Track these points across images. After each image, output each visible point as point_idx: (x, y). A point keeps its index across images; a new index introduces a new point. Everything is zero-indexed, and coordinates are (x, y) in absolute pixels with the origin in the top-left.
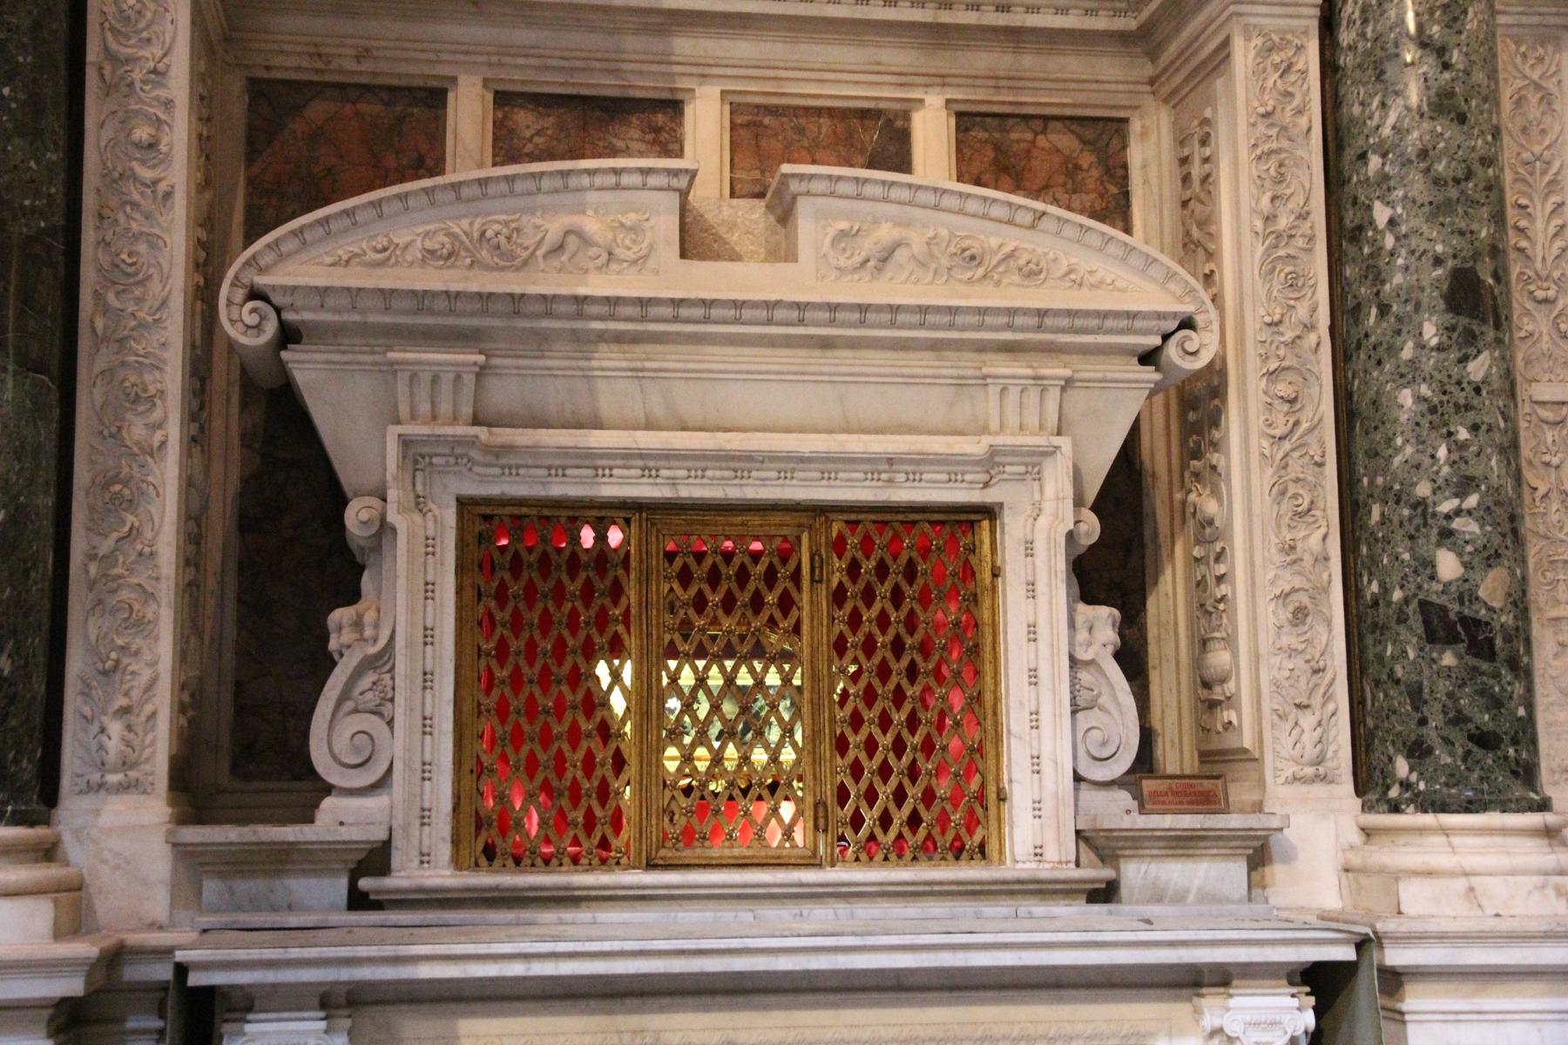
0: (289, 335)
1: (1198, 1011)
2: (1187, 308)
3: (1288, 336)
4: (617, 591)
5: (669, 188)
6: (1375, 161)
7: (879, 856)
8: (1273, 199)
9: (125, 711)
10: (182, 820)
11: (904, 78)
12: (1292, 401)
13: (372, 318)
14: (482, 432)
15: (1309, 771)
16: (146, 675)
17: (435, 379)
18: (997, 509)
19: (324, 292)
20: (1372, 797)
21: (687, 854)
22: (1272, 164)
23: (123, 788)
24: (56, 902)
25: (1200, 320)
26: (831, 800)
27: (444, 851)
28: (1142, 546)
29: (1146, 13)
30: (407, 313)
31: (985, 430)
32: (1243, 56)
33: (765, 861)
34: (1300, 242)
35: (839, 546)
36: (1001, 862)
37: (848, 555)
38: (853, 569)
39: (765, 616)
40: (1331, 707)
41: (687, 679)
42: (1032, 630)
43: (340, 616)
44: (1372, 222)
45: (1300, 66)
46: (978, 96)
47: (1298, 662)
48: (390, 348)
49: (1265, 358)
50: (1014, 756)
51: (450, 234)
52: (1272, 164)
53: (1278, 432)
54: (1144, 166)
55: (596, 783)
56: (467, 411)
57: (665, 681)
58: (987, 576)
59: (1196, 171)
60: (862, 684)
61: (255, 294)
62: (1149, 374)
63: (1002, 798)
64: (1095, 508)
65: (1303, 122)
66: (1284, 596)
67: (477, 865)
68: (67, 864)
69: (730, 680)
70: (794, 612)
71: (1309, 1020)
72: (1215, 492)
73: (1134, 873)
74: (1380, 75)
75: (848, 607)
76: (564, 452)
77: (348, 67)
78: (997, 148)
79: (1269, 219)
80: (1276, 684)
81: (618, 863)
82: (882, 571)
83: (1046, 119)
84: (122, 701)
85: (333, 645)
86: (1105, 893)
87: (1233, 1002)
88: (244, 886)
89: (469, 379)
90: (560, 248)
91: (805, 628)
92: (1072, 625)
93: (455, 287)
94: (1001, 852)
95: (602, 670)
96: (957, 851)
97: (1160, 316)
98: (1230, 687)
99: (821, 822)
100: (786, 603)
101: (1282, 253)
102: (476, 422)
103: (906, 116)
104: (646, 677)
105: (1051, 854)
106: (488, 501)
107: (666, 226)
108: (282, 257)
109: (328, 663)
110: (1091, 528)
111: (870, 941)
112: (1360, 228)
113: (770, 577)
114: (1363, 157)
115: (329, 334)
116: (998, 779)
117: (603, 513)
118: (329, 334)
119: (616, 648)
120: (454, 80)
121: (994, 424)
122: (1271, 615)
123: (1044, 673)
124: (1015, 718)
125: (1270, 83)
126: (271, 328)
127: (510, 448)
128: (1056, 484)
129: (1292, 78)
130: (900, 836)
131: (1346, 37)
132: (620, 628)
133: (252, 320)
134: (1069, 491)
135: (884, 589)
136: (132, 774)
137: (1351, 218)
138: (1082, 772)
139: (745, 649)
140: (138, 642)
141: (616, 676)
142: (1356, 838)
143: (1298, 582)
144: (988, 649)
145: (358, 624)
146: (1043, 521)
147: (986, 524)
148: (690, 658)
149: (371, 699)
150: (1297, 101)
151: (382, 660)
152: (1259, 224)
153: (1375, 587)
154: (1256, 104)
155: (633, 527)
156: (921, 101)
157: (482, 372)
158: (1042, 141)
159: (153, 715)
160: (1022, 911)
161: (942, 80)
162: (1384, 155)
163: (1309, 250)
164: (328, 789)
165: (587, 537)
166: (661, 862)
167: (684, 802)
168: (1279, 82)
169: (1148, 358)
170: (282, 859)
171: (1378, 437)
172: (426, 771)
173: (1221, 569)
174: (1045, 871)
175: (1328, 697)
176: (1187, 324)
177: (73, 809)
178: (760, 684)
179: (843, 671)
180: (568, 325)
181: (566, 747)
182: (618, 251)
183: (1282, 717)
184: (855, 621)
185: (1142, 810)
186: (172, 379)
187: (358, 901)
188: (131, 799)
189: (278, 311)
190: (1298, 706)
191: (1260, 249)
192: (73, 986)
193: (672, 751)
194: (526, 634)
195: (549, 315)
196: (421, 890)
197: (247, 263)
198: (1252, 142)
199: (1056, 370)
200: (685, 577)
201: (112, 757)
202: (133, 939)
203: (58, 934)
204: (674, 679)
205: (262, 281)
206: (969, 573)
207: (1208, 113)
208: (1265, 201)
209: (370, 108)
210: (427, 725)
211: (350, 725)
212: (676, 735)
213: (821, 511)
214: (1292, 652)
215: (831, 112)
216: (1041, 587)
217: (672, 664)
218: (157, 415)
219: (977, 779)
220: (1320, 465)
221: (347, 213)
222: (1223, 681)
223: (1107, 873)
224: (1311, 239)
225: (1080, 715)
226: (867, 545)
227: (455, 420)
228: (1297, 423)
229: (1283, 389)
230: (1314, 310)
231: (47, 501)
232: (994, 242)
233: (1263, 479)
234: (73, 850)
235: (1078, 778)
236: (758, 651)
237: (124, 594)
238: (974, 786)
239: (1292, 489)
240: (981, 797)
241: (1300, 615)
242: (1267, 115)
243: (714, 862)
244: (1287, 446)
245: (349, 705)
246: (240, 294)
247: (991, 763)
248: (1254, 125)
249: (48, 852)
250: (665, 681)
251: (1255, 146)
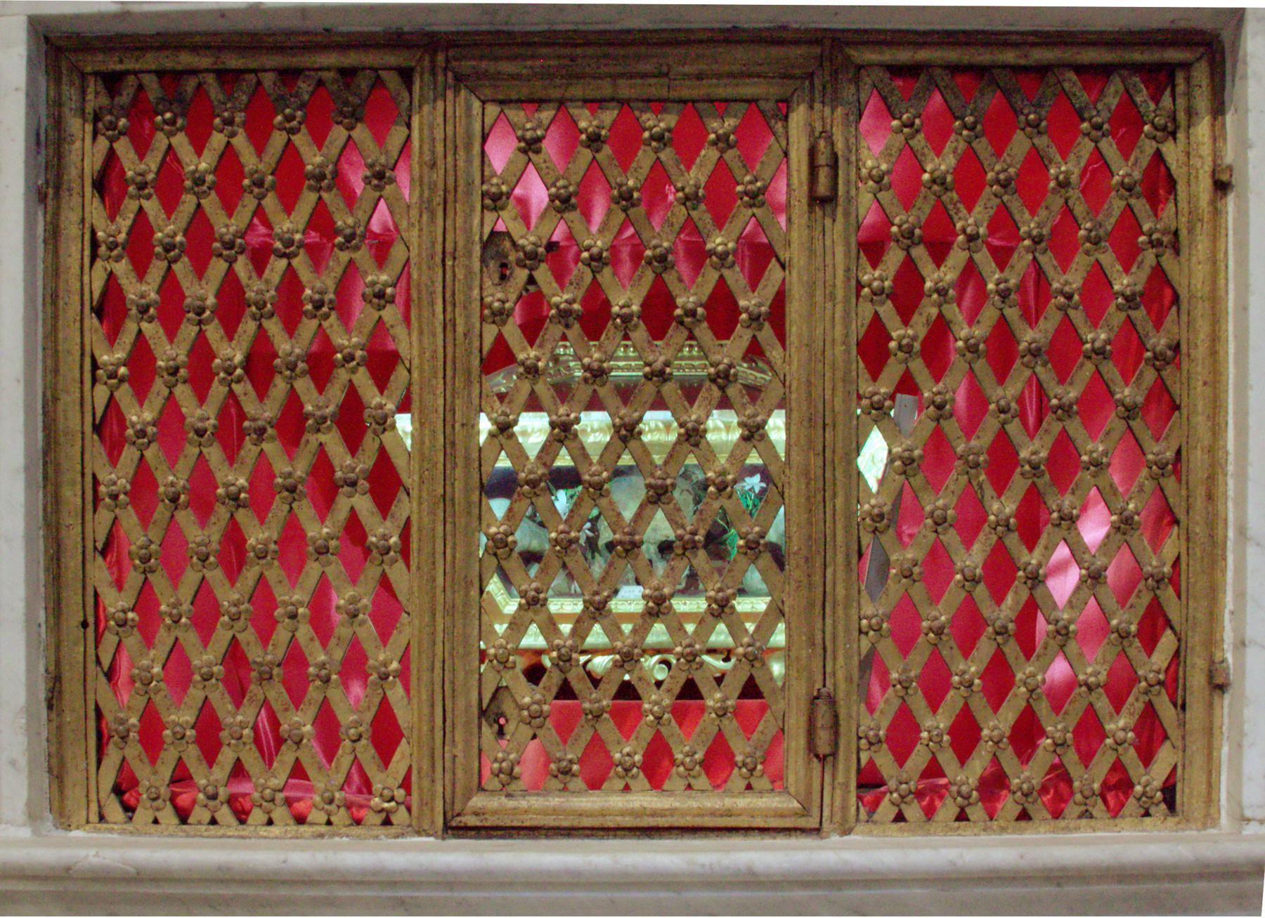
18: (1226, 36)
33: (698, 822)
36: (1210, 819)
50: (1252, 585)
55: (339, 654)
58: (1204, 187)
67: (102, 818)
70: (774, 274)
81: (387, 822)
94: (1210, 798)
99: (823, 737)
116: (1212, 641)
130: (933, 769)
144: (1201, 352)
147: (1201, 74)
155: (416, 87)
166: (472, 821)
167: (526, 695)
219: (1167, 642)
238: (1161, 657)
240: (1172, 682)
243: (587, 822)
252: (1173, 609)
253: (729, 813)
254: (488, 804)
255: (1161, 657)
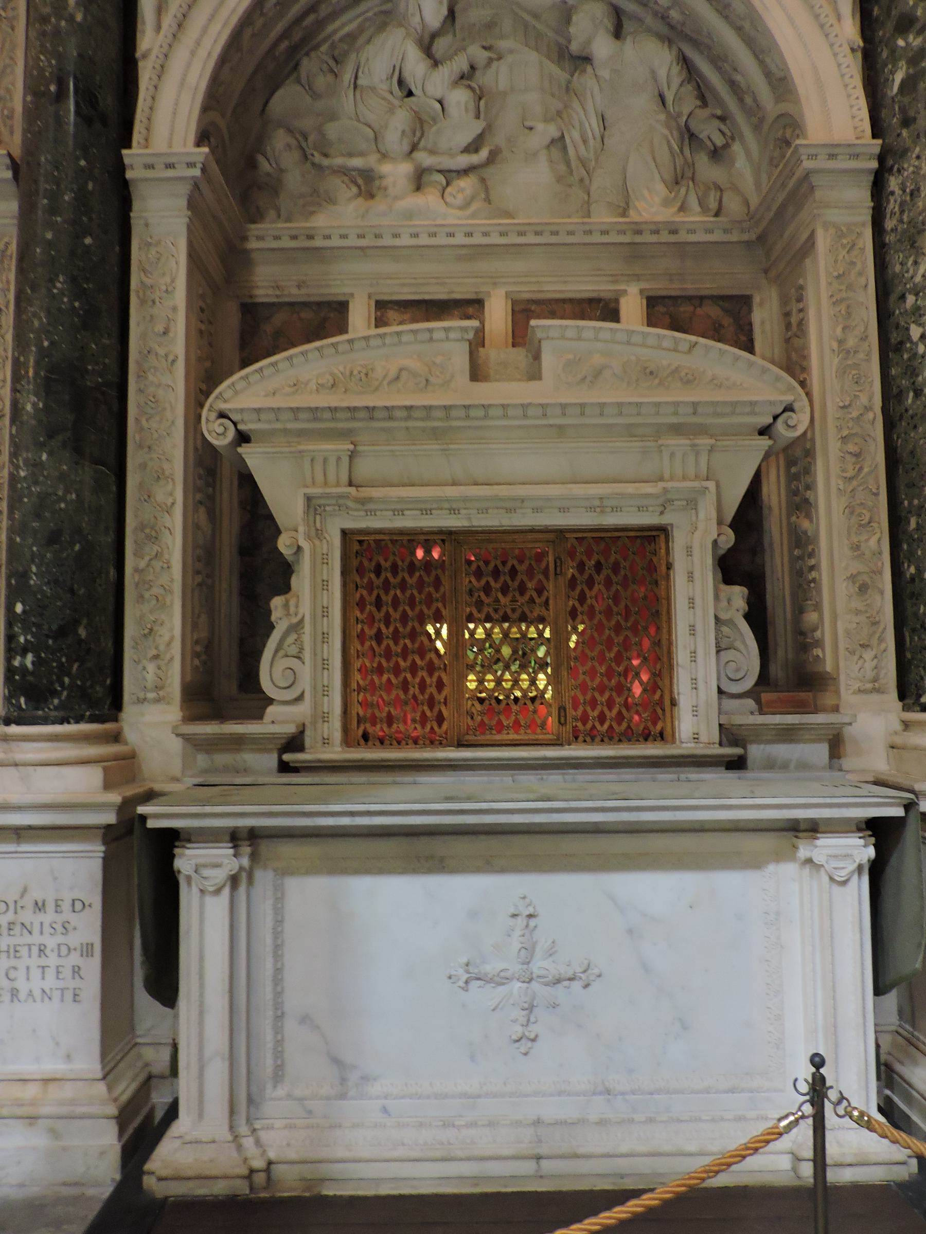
0: (243, 438)
1: (795, 847)
2: (789, 398)
3: (855, 414)
4: (437, 583)
5: (463, 339)
6: (910, 299)
7: (598, 739)
8: (844, 329)
9: (156, 657)
10: (190, 718)
11: (615, 278)
12: (857, 455)
13: (289, 426)
14: (352, 490)
15: (869, 686)
16: (167, 638)
17: (325, 461)
18: (669, 528)
19: (258, 411)
20: (909, 701)
21: (481, 738)
22: (843, 307)
23: (158, 700)
24: (105, 770)
25: (796, 406)
26: (569, 706)
27: (337, 735)
28: (763, 551)
29: (759, 230)
30: (309, 421)
31: (661, 479)
32: (822, 242)
33: (528, 742)
34: (861, 356)
35: (572, 554)
36: (674, 742)
37: (578, 559)
38: (581, 567)
39: (527, 597)
40: (883, 646)
41: (480, 633)
42: (691, 602)
43: (277, 602)
44: (909, 338)
45: (860, 245)
46: (660, 287)
47: (862, 618)
48: (299, 443)
49: (839, 429)
51: (332, 374)
52: (843, 307)
53: (848, 475)
54: (763, 323)
55: (427, 697)
56: (344, 479)
57: (467, 636)
58: (664, 568)
59: (794, 320)
60: (586, 637)
61: (222, 415)
62: (765, 443)
63: (674, 703)
64: (731, 526)
65: (862, 280)
66: (852, 578)
67: (359, 744)
68: (126, 744)
69: (506, 634)
70: (545, 593)
71: (871, 852)
72: (808, 516)
73: (755, 752)
74: (913, 245)
75: (579, 589)
76: (401, 500)
77: (294, 293)
78: (671, 316)
79: (841, 342)
80: (848, 633)
81: (441, 744)
82: (598, 567)
83: (702, 298)
84: (154, 652)
85: (273, 618)
86: (737, 764)
87: (819, 842)
88: (222, 759)
89: (345, 460)
90: (397, 378)
91: (551, 602)
92: (717, 597)
93: (334, 404)
95: (430, 629)
96: (646, 737)
97: (772, 403)
98: (818, 634)
99: (562, 719)
100: (540, 590)
101: (850, 362)
102: (350, 484)
103: (617, 301)
104: (455, 633)
105: (704, 738)
106: (361, 532)
107: (460, 360)
108: (236, 393)
109: (272, 627)
110: (728, 539)
111: (574, 804)
112: (901, 343)
113: (530, 572)
114: (903, 297)
115: (267, 435)
116: (671, 692)
117: (428, 538)
118: (267, 435)
119: (438, 618)
120: (352, 295)
121: (667, 475)
122: (843, 589)
123: (699, 627)
124: (681, 656)
125: (840, 257)
126: (231, 434)
127: (370, 500)
128: (707, 511)
129: (855, 252)
131: (889, 224)
132: (440, 605)
133: (220, 430)
134: (714, 515)
135: (601, 578)
136: (161, 693)
137: (894, 337)
138: (724, 688)
139: (516, 615)
140: (163, 617)
141: (438, 632)
142: (898, 727)
143: (862, 568)
144: (664, 613)
145: (286, 606)
146: (698, 534)
147: (663, 537)
148: (479, 622)
149: (293, 650)
150: (859, 266)
151: (296, 627)
152: (835, 346)
153: (912, 570)
154: (832, 270)
155: (446, 544)
156: (625, 291)
157: (353, 455)
158: (699, 311)
159: (172, 659)
160: (683, 776)
161: (638, 278)
162: (917, 295)
163: (868, 361)
164: (270, 701)
165: (420, 553)
166: (466, 743)
168: (846, 256)
169: (764, 431)
170: (238, 743)
171: (914, 474)
172: (326, 691)
173: (813, 562)
174: (700, 750)
175: (881, 640)
176: (789, 408)
177: (130, 712)
178: (524, 635)
179: (575, 629)
180: (403, 424)
181: (409, 676)
182: (431, 379)
183: (853, 653)
184: (582, 599)
185: (761, 712)
186: (177, 466)
187: (284, 768)
188: (161, 707)
189: (235, 424)
190: (862, 646)
191: (836, 361)
192: (110, 818)
193: (471, 677)
194: (384, 609)
195: (391, 418)
196: (320, 761)
197: (217, 397)
198: (830, 294)
199: (704, 442)
200: (479, 574)
201: (149, 685)
202: (157, 787)
203: (108, 786)
204: (472, 633)
205: (223, 406)
206: (652, 568)
207: (801, 282)
208: (839, 330)
209: (306, 314)
210: (325, 664)
211: (282, 663)
212: (471, 667)
213: (560, 533)
214: (857, 612)
215: (571, 301)
216: (697, 575)
217: (471, 626)
218: (170, 487)
219: (659, 693)
220: (876, 494)
221: (273, 365)
222: (815, 630)
223: (738, 751)
224: (869, 354)
225: (722, 653)
226: (589, 553)
227: (338, 484)
228: (861, 469)
229: (851, 448)
230: (871, 399)
231: (110, 538)
232: (665, 363)
233: (838, 505)
234: (130, 734)
235: (720, 692)
236: (523, 618)
237: (155, 590)
238: (657, 696)
239: (858, 510)
240: (661, 702)
241: (863, 589)
242: (839, 277)
243: (497, 743)
244: (855, 483)
245: (281, 653)
246: (213, 415)
247: (667, 681)
248: (830, 284)
249: (116, 738)
250: (467, 636)
251: (832, 296)
252: (660, 683)
253: (537, 740)
254: (470, 738)
255: (657, 696)
